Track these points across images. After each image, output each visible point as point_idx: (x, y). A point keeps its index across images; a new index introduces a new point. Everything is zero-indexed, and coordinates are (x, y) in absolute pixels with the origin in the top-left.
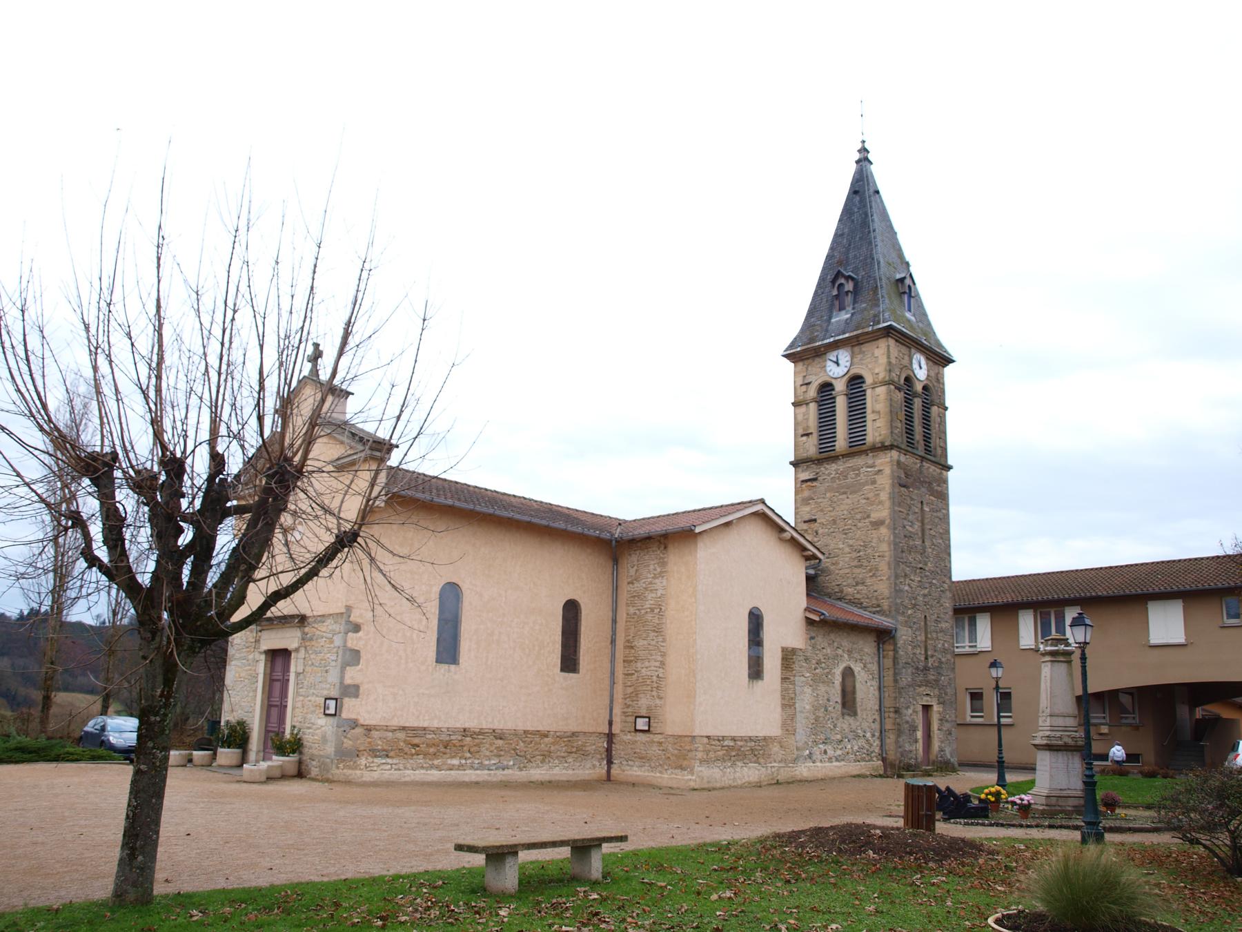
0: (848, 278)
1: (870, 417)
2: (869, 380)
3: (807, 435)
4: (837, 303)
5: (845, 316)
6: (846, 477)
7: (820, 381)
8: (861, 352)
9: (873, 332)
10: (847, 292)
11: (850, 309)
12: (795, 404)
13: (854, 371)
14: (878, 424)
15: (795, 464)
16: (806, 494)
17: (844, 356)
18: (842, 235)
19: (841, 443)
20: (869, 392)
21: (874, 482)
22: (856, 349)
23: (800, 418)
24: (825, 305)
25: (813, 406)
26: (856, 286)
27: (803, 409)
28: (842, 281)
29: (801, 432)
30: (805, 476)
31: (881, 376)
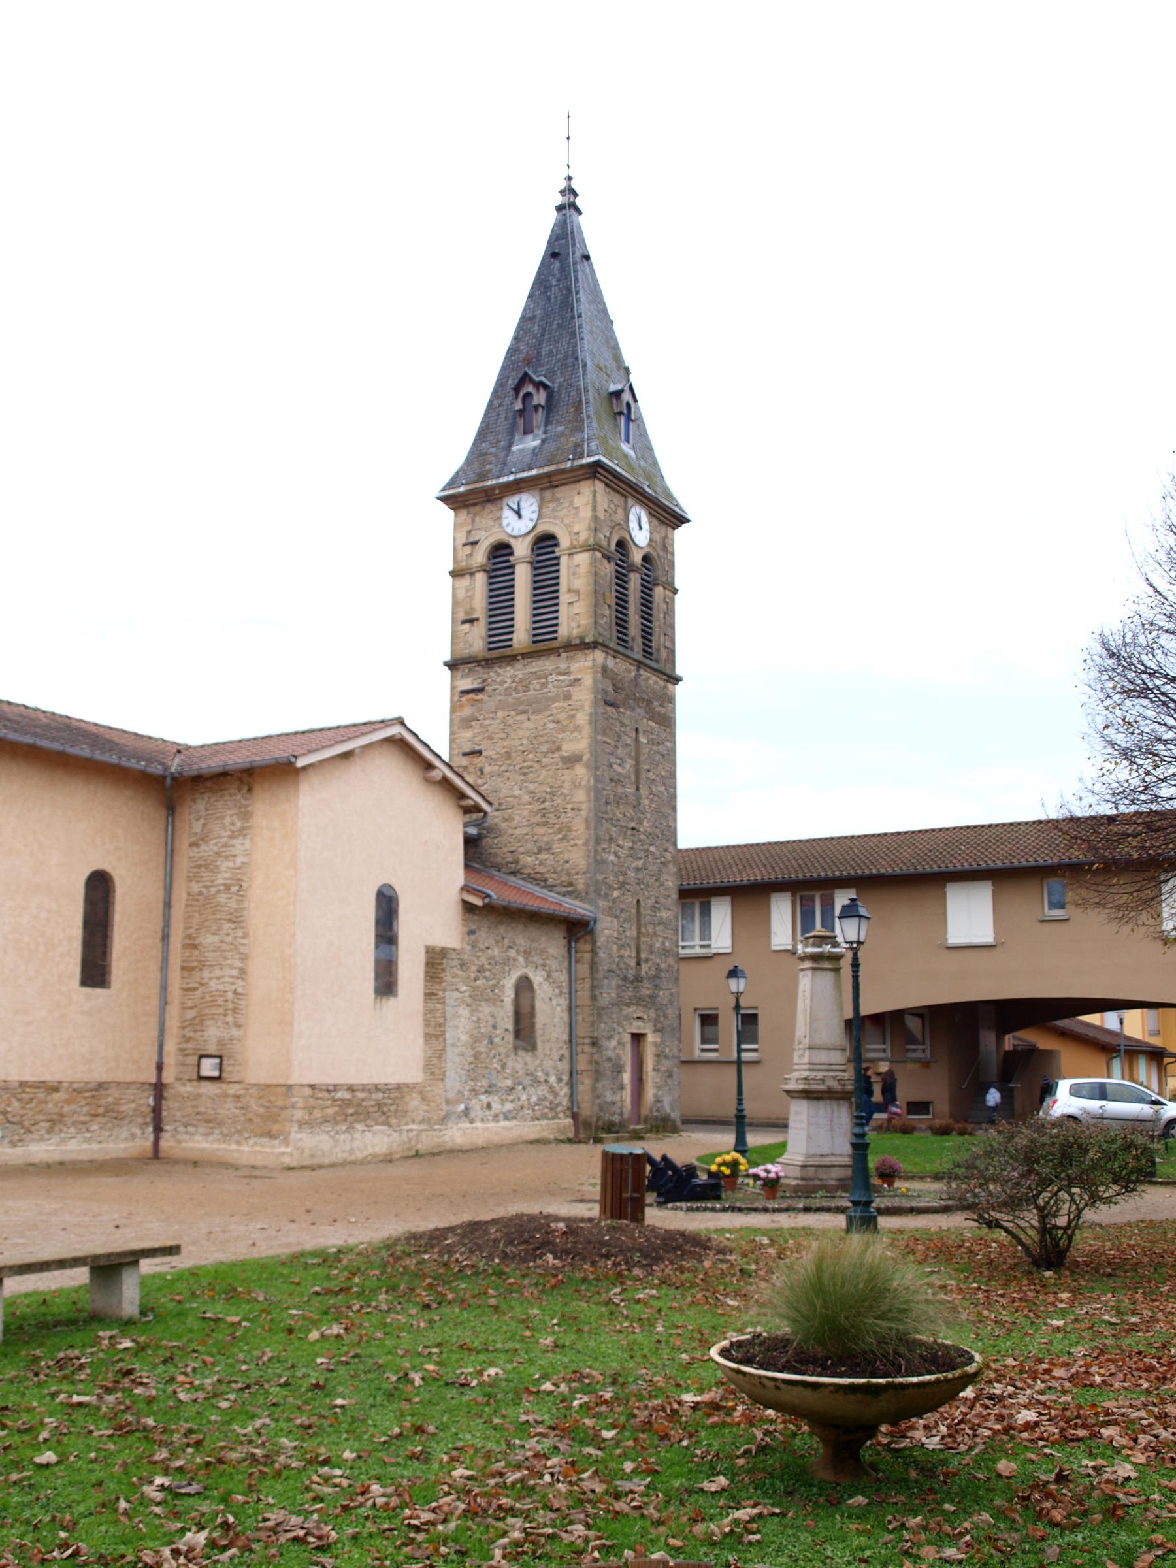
0: (539, 385)
1: (564, 598)
2: (564, 542)
3: (471, 621)
4: (520, 422)
5: (532, 442)
7: (492, 540)
8: (555, 499)
9: (573, 469)
10: (536, 407)
11: (539, 432)
12: (455, 574)
13: (543, 527)
14: (576, 609)
15: (452, 665)
16: (467, 711)
17: (529, 503)
18: (534, 317)
19: (521, 635)
20: (564, 561)
21: (567, 697)
22: (548, 494)
23: (461, 594)
24: (503, 425)
25: (481, 579)
26: (550, 398)
27: (465, 582)
28: (530, 388)
29: (462, 616)
30: (467, 684)
31: (583, 536)
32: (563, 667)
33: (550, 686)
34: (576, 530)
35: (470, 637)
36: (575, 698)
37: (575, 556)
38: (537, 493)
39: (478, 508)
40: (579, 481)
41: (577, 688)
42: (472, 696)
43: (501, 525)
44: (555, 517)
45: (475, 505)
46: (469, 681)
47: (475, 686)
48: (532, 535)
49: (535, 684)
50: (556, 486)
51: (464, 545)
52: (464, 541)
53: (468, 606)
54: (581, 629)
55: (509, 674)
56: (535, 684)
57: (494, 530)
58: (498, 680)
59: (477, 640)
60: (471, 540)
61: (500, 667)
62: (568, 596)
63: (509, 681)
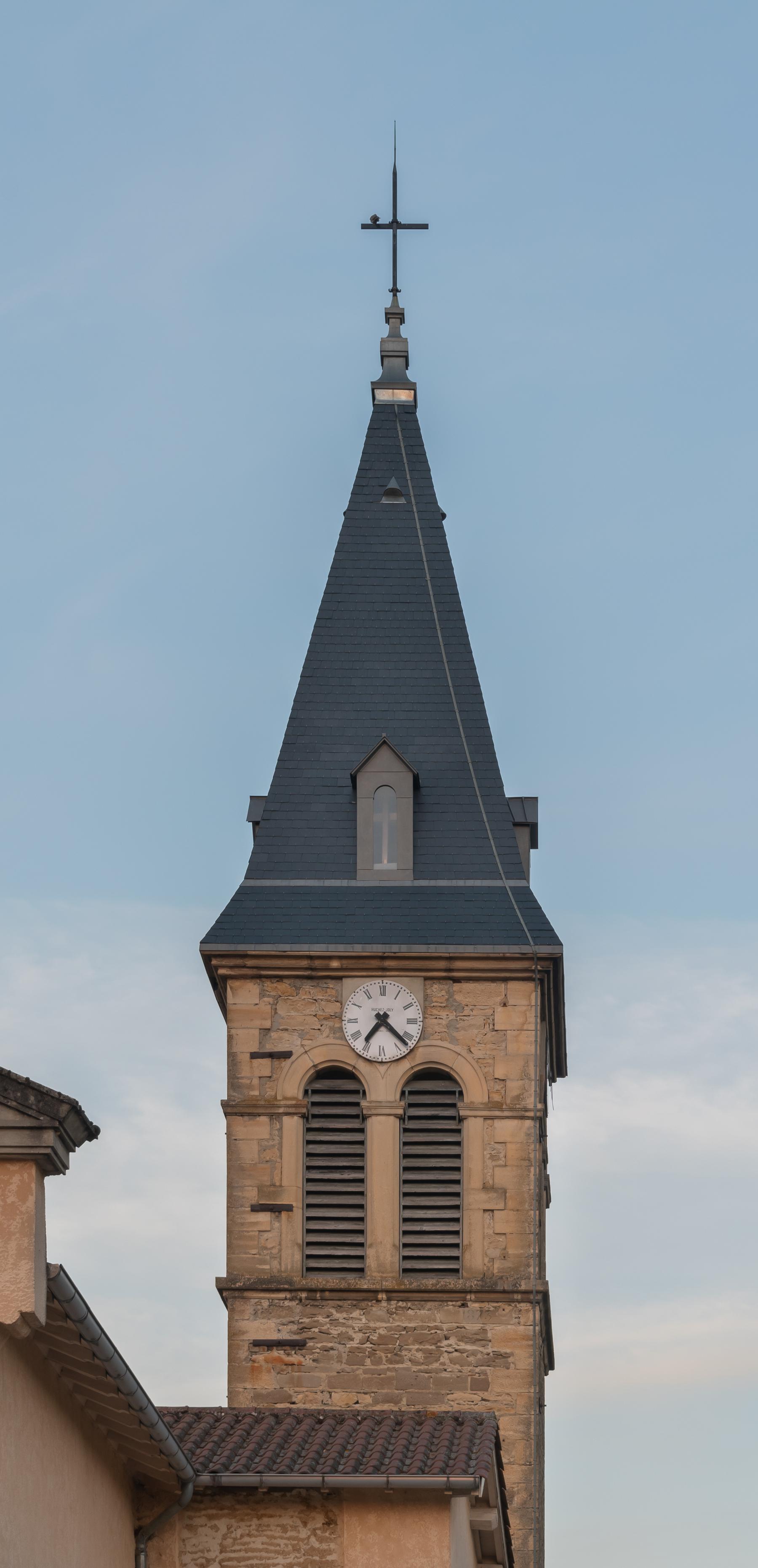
1: (474, 1199)
2: (475, 1090)
3: (276, 1210)
6: (396, 1357)
8: (450, 1004)
15: (229, 1290)
16: (268, 1382)
20: (473, 1129)
21: (481, 1384)
22: (438, 991)
25: (293, 1126)
27: (261, 1128)
29: (251, 1195)
32: (473, 1327)
33: (445, 1358)
34: (499, 1074)
35: (270, 1240)
36: (495, 1388)
37: (498, 1123)
38: (418, 983)
39: (284, 986)
40: (505, 980)
41: (501, 1372)
42: (276, 1353)
43: (339, 1032)
44: (454, 1041)
45: (280, 978)
46: (272, 1323)
47: (285, 1336)
48: (406, 1065)
49: (414, 1351)
50: (457, 980)
51: (254, 1056)
52: (255, 1049)
53: (266, 1180)
54: (508, 1264)
55: (357, 1325)
56: (414, 1351)
57: (322, 1039)
58: (335, 1332)
59: (283, 1244)
60: (269, 1048)
61: (339, 1308)
62: (483, 1196)
63: (358, 1337)
